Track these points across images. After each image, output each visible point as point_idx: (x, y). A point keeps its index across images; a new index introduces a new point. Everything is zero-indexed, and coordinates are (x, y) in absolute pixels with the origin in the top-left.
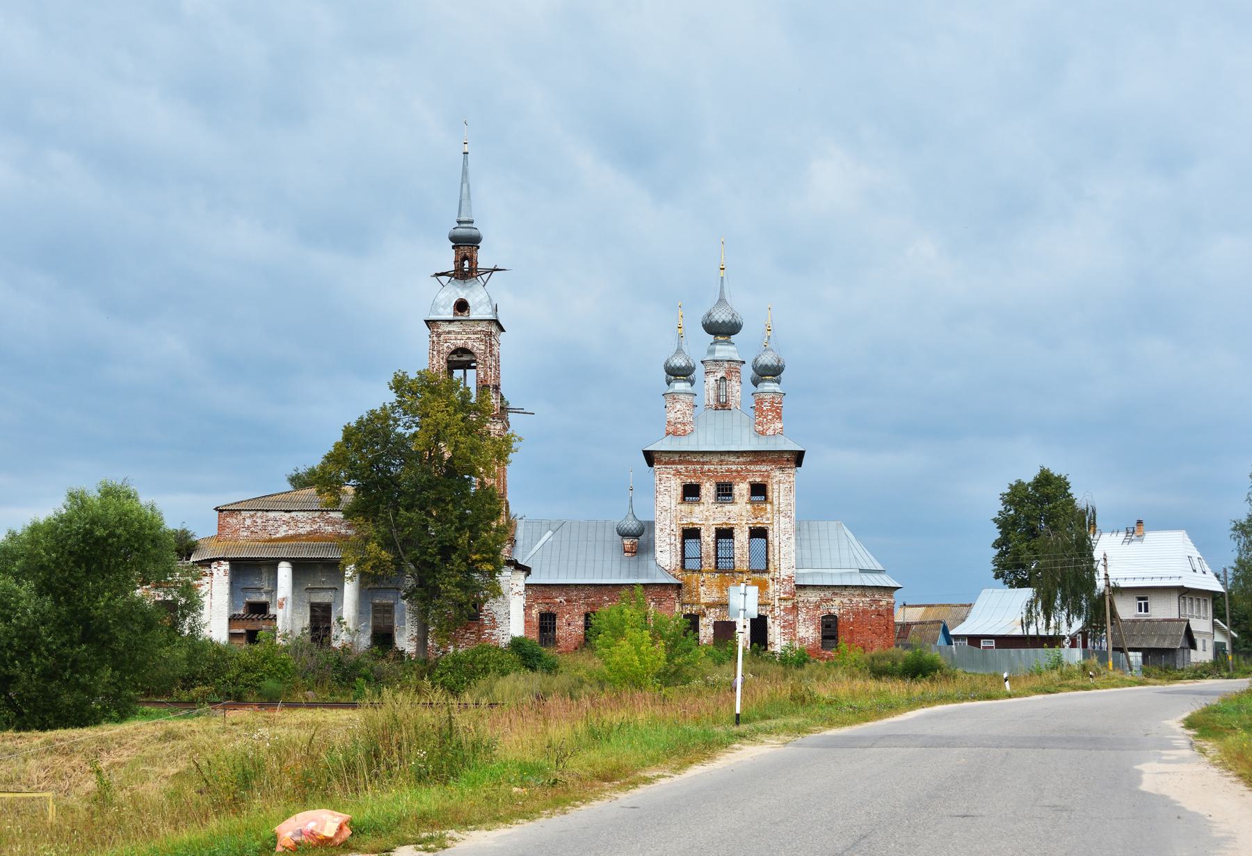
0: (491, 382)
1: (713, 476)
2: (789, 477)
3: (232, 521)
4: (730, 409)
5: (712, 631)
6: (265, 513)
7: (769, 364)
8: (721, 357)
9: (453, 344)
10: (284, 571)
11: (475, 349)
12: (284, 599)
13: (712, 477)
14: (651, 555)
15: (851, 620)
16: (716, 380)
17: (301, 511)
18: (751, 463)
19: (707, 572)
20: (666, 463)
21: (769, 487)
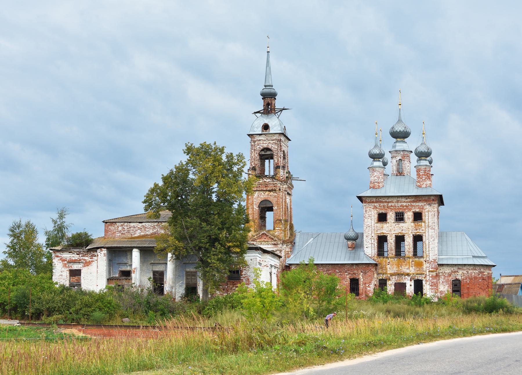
0: (281, 164)
1: (393, 209)
2: (434, 208)
3: (112, 228)
4: (404, 175)
5: (394, 288)
6: (129, 223)
7: (423, 151)
8: (399, 149)
9: (261, 146)
10: (136, 254)
11: (273, 148)
12: (135, 269)
13: (393, 209)
14: (362, 249)
15: (468, 282)
16: (397, 161)
17: (147, 222)
18: (414, 202)
19: (391, 258)
20: (369, 203)
21: (423, 214)
